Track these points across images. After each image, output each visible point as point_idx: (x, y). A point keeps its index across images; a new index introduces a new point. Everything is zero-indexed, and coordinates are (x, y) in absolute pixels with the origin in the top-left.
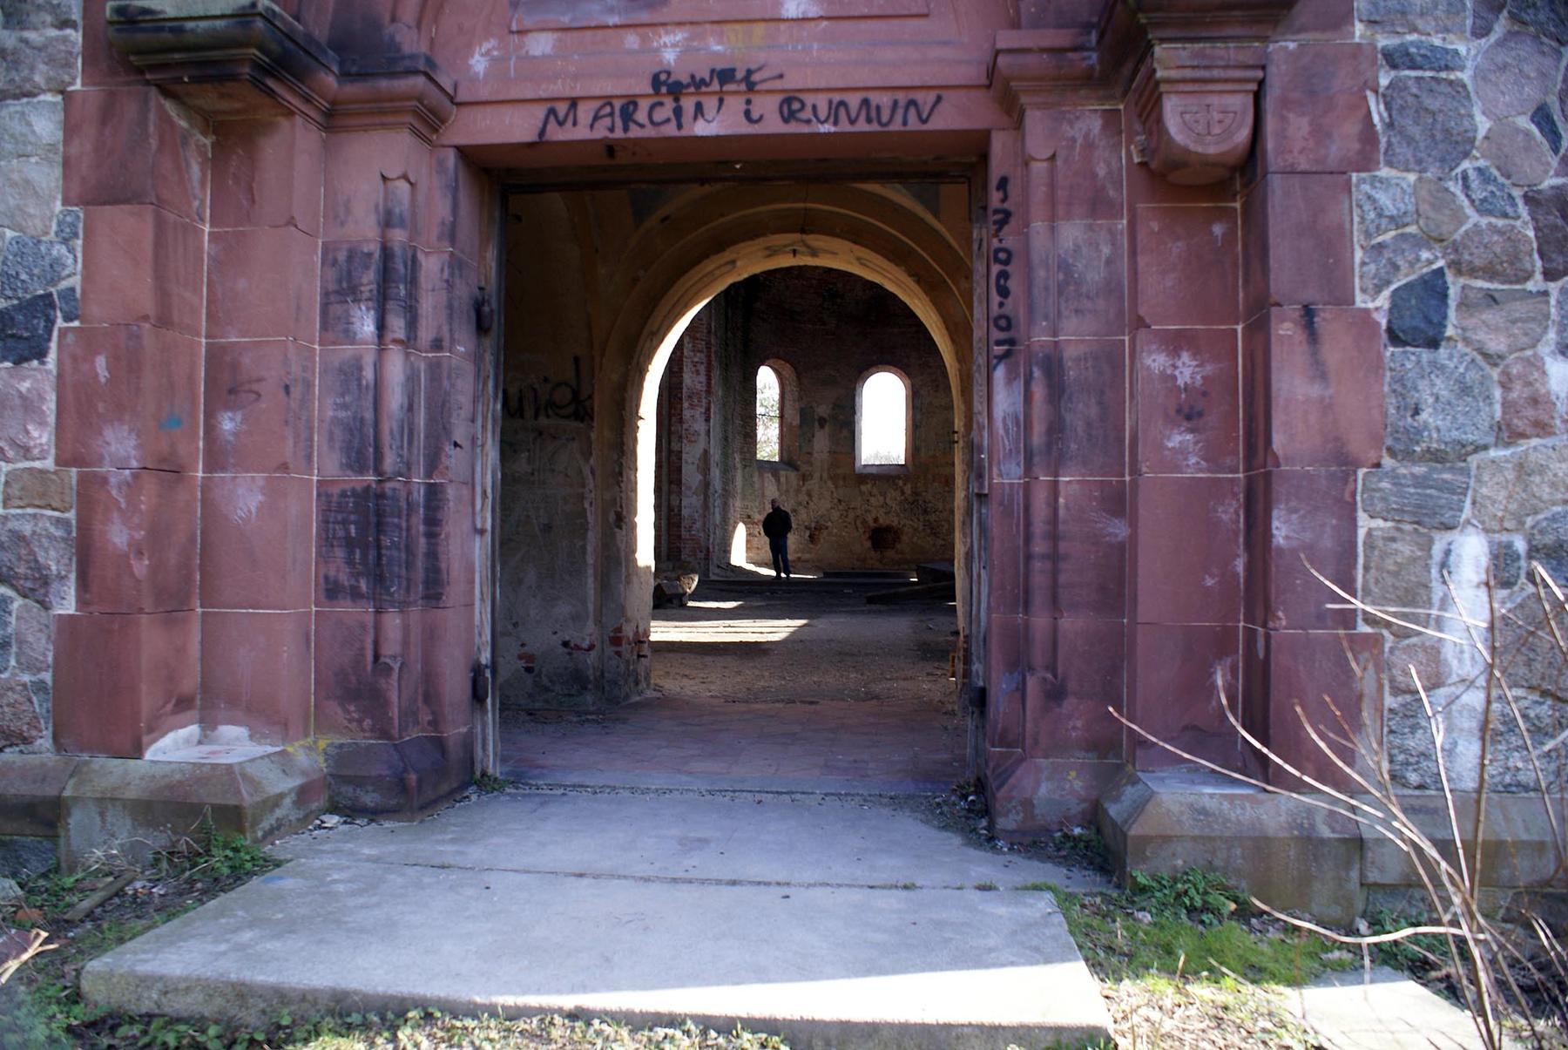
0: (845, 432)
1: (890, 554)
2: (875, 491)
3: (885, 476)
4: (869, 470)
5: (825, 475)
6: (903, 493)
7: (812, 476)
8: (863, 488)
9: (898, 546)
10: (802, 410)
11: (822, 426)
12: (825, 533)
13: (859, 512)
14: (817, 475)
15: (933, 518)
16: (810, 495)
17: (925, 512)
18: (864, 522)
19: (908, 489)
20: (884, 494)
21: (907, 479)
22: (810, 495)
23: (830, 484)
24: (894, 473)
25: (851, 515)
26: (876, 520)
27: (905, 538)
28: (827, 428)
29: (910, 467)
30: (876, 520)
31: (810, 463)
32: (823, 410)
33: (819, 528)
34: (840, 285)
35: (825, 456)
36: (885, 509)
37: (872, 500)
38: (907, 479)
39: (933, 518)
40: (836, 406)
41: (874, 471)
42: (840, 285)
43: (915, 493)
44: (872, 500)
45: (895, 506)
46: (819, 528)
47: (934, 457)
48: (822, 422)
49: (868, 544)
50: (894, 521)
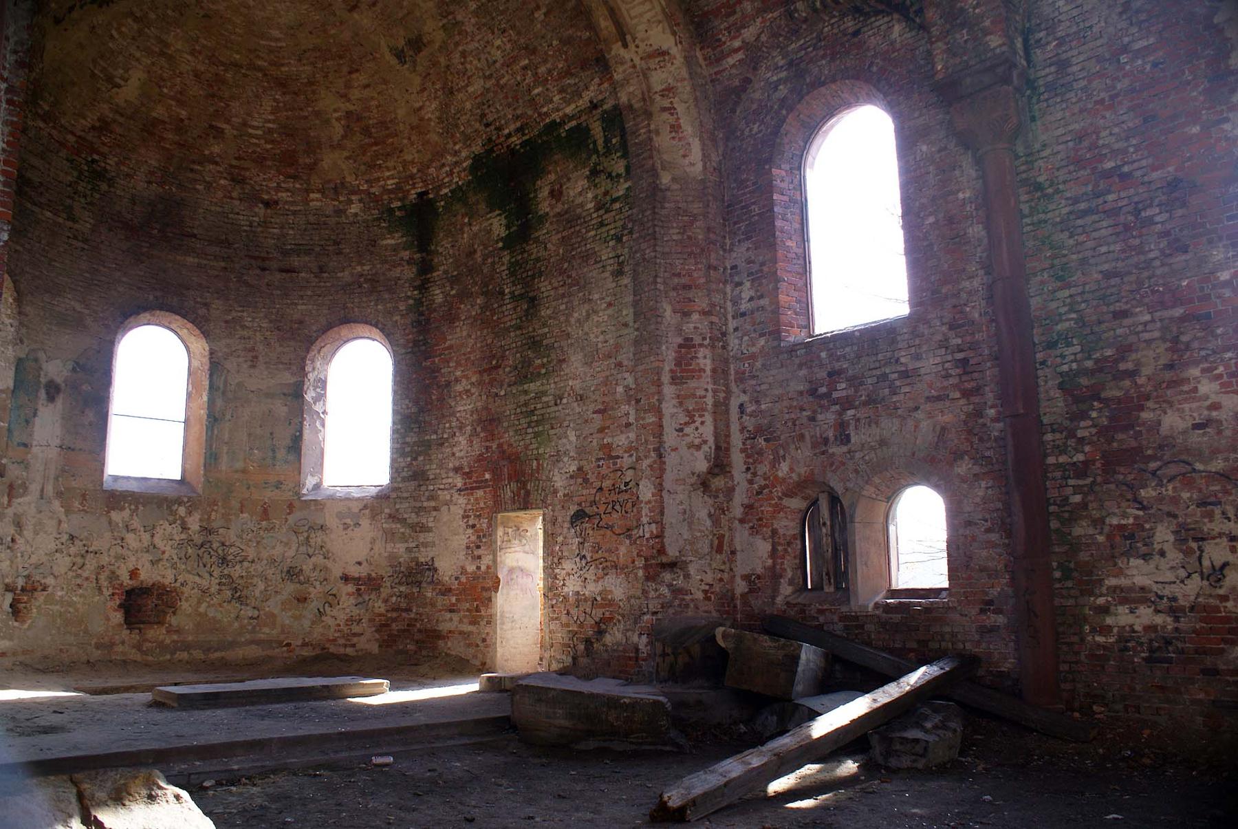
0: (91, 415)
1: (156, 633)
2: (136, 523)
3: (149, 500)
4: (121, 486)
5: (50, 489)
6: (185, 528)
7: (25, 487)
8: (116, 516)
9: (174, 620)
10: (20, 364)
11: (51, 399)
12: (41, 597)
13: (105, 560)
14: (34, 488)
15: (237, 571)
16: (19, 525)
17: (224, 561)
18: (113, 576)
19: (194, 523)
20: (151, 529)
21: (193, 505)
22: (19, 525)
23: (56, 504)
24: (171, 493)
25: (91, 563)
26: (134, 574)
27: (184, 605)
28: (60, 401)
29: (198, 482)
30: (134, 574)
31: (24, 464)
32: (55, 369)
33: (31, 589)
34: (112, 161)
35: (53, 453)
36: (151, 557)
37: (130, 537)
38: (193, 505)
39: (237, 571)
40: (78, 367)
41: (133, 487)
42: (112, 161)
43: (207, 530)
44: (130, 537)
45: (170, 551)
46: (31, 589)
47: (244, 471)
48: (53, 391)
49: (118, 617)
50: (165, 576)
